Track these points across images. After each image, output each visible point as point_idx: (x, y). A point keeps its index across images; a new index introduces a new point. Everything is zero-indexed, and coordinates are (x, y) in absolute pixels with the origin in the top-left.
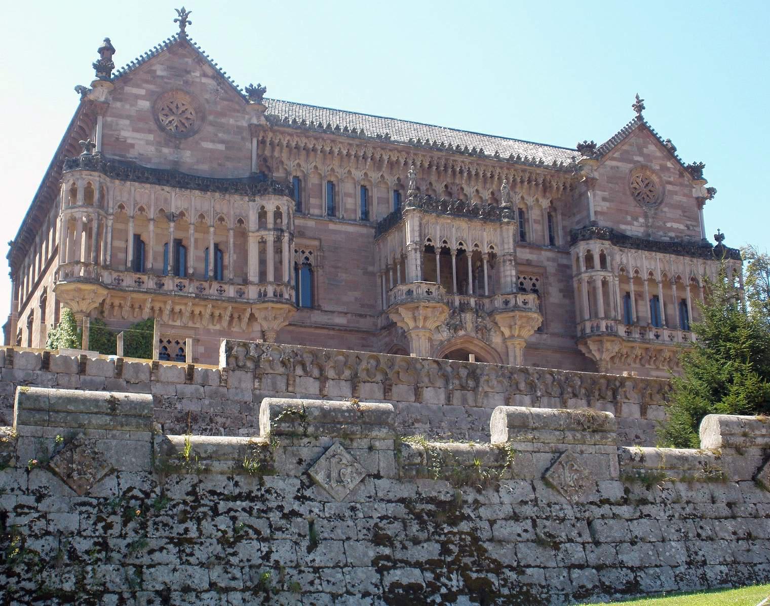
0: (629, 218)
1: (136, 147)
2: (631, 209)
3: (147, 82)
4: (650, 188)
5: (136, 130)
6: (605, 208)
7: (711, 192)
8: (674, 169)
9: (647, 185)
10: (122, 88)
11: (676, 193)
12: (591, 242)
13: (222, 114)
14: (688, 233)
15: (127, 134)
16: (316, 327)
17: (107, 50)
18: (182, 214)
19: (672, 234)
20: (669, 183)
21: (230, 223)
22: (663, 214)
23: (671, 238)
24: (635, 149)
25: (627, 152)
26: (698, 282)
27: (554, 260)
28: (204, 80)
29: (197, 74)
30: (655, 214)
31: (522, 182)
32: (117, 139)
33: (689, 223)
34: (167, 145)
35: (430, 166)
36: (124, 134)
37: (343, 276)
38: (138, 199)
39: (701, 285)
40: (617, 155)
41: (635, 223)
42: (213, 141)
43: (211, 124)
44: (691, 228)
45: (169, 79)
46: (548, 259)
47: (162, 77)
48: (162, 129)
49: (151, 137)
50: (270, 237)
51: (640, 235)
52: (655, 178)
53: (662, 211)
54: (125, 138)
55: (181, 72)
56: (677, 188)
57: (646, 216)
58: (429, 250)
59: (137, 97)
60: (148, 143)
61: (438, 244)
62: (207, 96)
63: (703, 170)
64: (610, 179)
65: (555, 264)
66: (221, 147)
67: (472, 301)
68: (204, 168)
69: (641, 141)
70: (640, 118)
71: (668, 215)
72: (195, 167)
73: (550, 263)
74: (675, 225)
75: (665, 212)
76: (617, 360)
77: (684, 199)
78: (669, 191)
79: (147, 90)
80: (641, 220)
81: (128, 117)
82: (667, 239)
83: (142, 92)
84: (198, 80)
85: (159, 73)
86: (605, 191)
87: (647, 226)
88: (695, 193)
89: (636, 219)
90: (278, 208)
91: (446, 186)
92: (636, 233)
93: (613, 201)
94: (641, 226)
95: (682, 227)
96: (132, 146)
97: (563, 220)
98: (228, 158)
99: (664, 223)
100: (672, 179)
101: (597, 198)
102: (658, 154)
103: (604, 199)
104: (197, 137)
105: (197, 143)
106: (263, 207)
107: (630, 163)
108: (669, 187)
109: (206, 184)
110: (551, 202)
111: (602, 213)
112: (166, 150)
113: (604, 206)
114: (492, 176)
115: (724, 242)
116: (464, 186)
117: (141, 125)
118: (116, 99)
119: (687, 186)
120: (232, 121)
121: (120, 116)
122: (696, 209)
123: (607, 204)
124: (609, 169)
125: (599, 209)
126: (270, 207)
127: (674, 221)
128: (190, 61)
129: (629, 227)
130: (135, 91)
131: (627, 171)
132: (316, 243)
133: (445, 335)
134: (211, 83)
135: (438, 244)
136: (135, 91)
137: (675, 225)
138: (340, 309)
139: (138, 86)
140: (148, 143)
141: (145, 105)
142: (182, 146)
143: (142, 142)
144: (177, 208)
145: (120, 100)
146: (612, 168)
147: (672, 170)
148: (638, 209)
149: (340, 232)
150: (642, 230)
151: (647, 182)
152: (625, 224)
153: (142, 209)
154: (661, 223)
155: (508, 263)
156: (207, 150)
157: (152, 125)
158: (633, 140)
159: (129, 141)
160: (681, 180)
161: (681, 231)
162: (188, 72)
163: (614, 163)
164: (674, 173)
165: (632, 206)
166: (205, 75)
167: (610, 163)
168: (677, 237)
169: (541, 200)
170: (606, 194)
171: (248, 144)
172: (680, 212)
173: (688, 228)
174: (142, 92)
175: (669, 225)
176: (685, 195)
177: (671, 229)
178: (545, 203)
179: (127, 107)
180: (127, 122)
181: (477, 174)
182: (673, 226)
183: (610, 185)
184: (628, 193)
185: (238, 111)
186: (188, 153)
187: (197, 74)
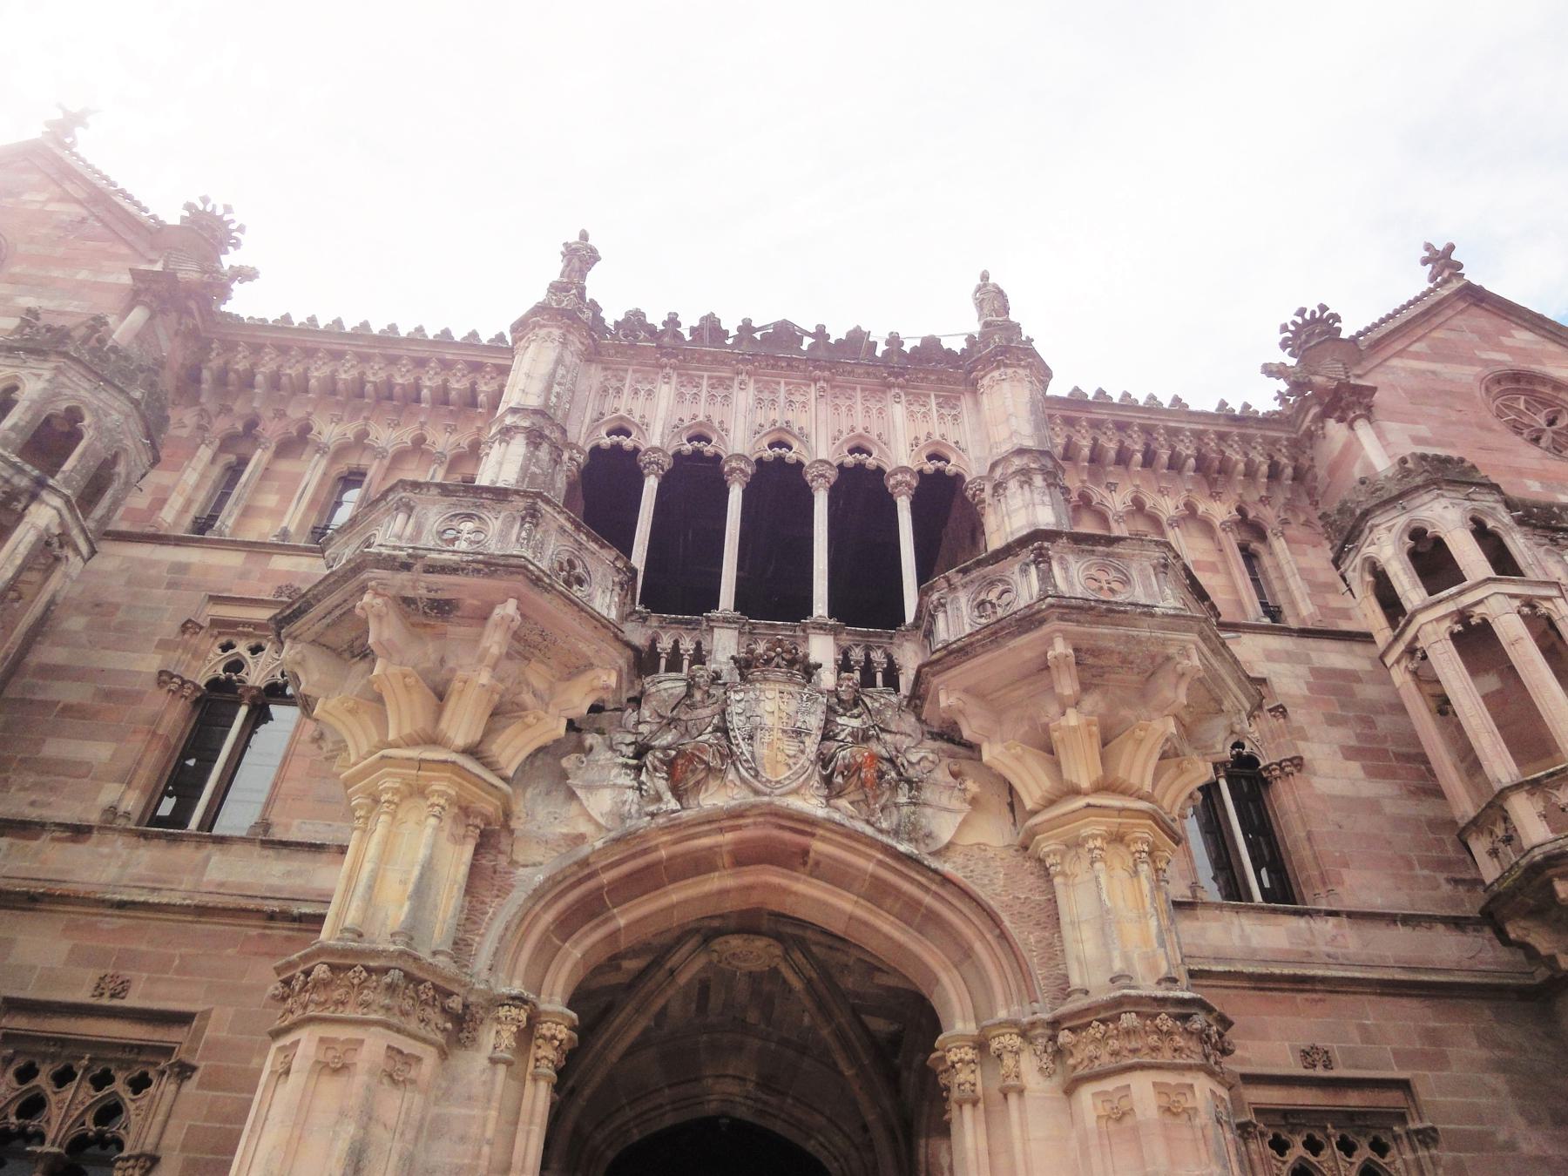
27: (1290, 657)
46: (1270, 656)
65: (1302, 670)
67: (821, 649)
73: (1277, 667)
133: (607, 800)
155: (1013, 485)
178: (1220, 511)
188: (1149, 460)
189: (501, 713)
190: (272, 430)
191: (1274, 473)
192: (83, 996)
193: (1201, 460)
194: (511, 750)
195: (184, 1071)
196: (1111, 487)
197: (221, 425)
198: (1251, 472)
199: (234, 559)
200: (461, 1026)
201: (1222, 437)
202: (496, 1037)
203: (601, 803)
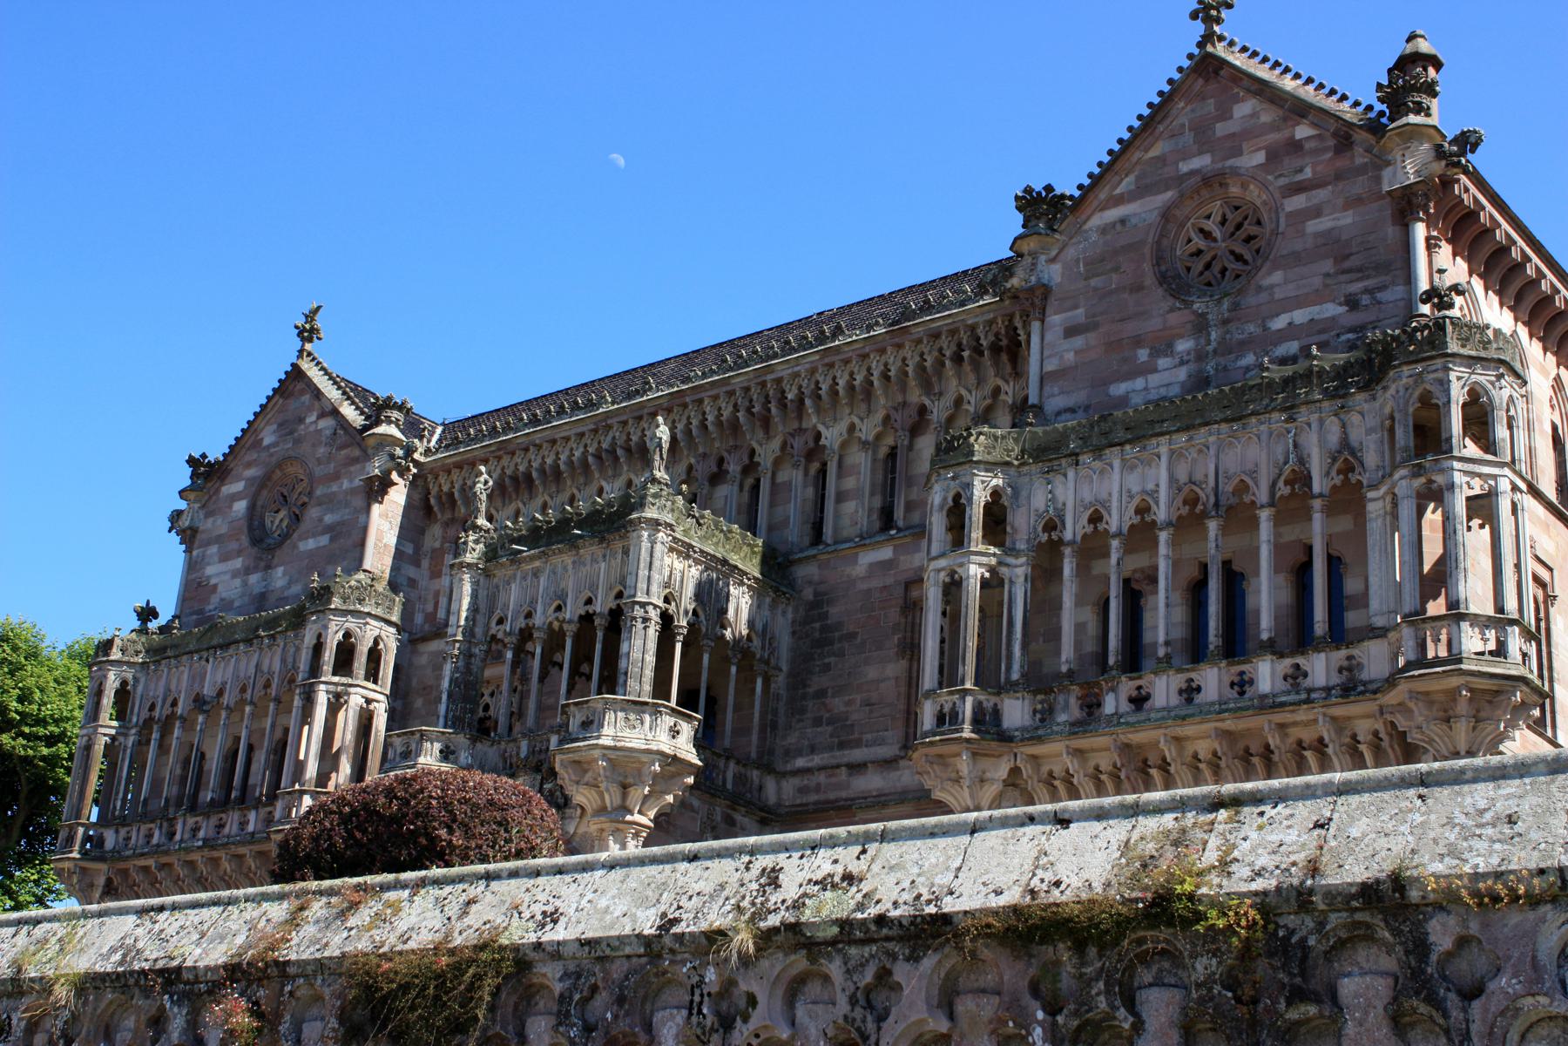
0: (1143, 354)
1: (220, 588)
2: (1155, 323)
3: (249, 465)
5: (224, 558)
6: (1070, 356)
11: (1317, 212)
13: (336, 477)
20: (1299, 188)
22: (1264, 297)
24: (1189, 137)
25: (1162, 160)
28: (322, 424)
30: (1235, 307)
32: (199, 584)
33: (1356, 287)
34: (256, 569)
40: (1127, 184)
41: (1163, 362)
49: (238, 563)
52: (1255, 194)
53: (1260, 289)
54: (209, 578)
56: (1322, 194)
57: (1200, 326)
59: (234, 498)
60: (235, 574)
64: (1095, 265)
66: (324, 540)
71: (1279, 294)
74: (1300, 316)
75: (1272, 287)
77: (1347, 219)
78: (1290, 215)
79: (248, 480)
92: (1153, 395)
94: (1182, 363)
95: (1332, 310)
100: (1308, 173)
101: (1048, 337)
103: (1071, 332)
105: (295, 547)
107: (1167, 189)
108: (1297, 202)
113: (1067, 352)
116: (821, 428)
117: (234, 546)
118: (208, 515)
119: (1362, 170)
120: (346, 484)
121: (208, 543)
122: (1392, 231)
123: (1078, 341)
124: (1094, 237)
125: (1050, 367)
129: (1139, 383)
131: (1153, 217)
141: (241, 506)
142: (276, 561)
146: (1104, 230)
147: (1307, 146)
148: (1174, 319)
150: (1182, 374)
154: (1251, 328)
157: (245, 540)
158: (1183, 113)
159: (213, 582)
160: (1341, 163)
162: (301, 420)
164: (1316, 152)
165: (1160, 312)
166: (322, 415)
167: (1097, 220)
170: (1079, 314)
172: (1328, 266)
173: (1352, 303)
175: (1279, 323)
176: (1354, 202)
177: (1291, 331)
181: (834, 392)
183: (1093, 282)
184: (1150, 280)
186: (280, 570)
193: (996, 349)
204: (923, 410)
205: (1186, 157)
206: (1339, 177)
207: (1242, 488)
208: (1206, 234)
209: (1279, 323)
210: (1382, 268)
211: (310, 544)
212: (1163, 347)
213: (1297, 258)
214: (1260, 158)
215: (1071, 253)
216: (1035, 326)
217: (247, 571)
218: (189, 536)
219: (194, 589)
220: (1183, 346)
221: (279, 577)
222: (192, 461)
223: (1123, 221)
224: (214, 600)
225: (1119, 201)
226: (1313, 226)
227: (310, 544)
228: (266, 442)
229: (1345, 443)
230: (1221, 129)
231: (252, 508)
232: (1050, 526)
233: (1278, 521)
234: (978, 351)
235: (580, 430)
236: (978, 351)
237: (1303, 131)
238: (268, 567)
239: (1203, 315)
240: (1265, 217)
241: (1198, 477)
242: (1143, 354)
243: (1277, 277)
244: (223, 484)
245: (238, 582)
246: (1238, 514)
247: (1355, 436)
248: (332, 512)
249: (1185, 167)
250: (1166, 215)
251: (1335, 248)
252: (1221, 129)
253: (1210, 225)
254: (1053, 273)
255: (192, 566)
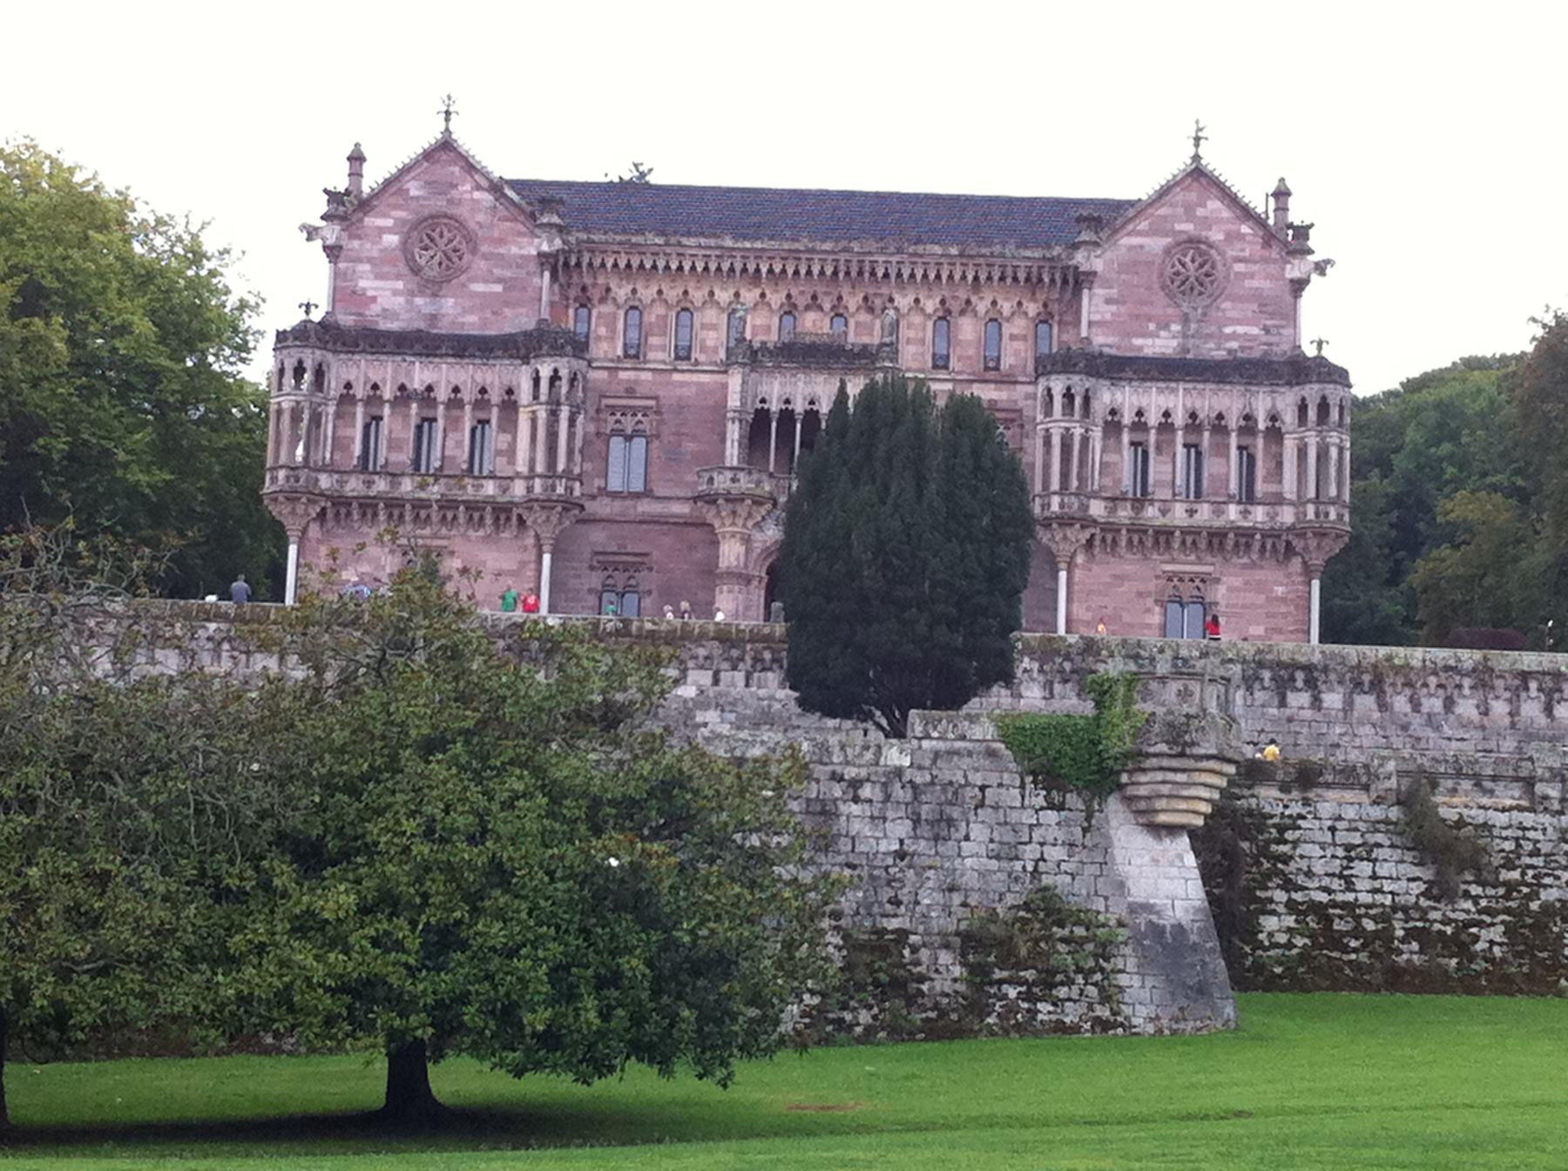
0: (1152, 326)
2: (1159, 311)
3: (396, 207)
4: (1207, 267)
5: (378, 277)
7: (1321, 268)
8: (1255, 235)
9: (1201, 266)
10: (361, 220)
11: (1252, 276)
12: (1053, 377)
13: (501, 241)
14: (1265, 339)
15: (366, 284)
16: (641, 522)
17: (357, 159)
18: (430, 388)
19: (1234, 345)
21: (495, 396)
23: (1230, 351)
24: (1180, 210)
25: (1165, 217)
26: (1256, 421)
28: (477, 195)
29: (468, 187)
30: (1205, 314)
31: (989, 278)
33: (1269, 323)
34: (422, 293)
35: (835, 273)
36: (362, 284)
37: (689, 446)
38: (370, 375)
39: (1261, 426)
40: (1143, 225)
41: (1163, 333)
42: (486, 281)
43: (485, 257)
44: (1273, 331)
45: (425, 199)
47: (417, 198)
48: (416, 270)
49: (400, 285)
50: (542, 415)
51: (1170, 351)
53: (1218, 308)
55: (441, 188)
56: (1255, 268)
57: (1185, 320)
58: (762, 416)
59: (382, 230)
60: (395, 293)
61: (775, 406)
62: (481, 217)
63: (1311, 232)
64: (1125, 267)
66: (498, 288)
68: (471, 323)
69: (1193, 196)
70: (1196, 158)
71: (1229, 314)
72: (461, 320)
74: (1240, 329)
76: (1097, 551)
77: (1267, 284)
80: (1175, 327)
81: (370, 260)
82: (1220, 354)
83: (389, 222)
84: (467, 196)
85: (413, 192)
86: (1111, 287)
87: (1185, 336)
88: (1294, 271)
89: (1166, 327)
90: (556, 371)
91: (866, 299)
92: (1157, 350)
93: (1124, 303)
95: (1255, 331)
96: (374, 299)
97: (1060, 331)
98: (507, 304)
99: (1220, 328)
100: (1247, 254)
102: (1226, 214)
103: (1108, 301)
104: (463, 278)
105: (464, 285)
106: (537, 372)
107: (1167, 235)
109: (465, 347)
110: (1045, 305)
111: (1100, 324)
112: (419, 301)
113: (1107, 312)
114: (938, 277)
115: (1325, 353)
117: (386, 269)
118: (351, 237)
119: (1275, 261)
120: (514, 250)
122: (1289, 298)
123: (1114, 308)
124: (1124, 250)
125: (1097, 317)
126: (545, 372)
127: (1239, 322)
128: (457, 169)
129: (1149, 341)
130: (381, 222)
132: (652, 403)
134: (486, 198)
135: (775, 406)
136: (381, 222)
137: (1240, 329)
138: (681, 495)
139: (385, 216)
140: (395, 293)
141: (392, 240)
143: (388, 293)
144: (422, 381)
145: (359, 237)
146: (1130, 248)
148: (1170, 311)
149: (687, 384)
150: (1174, 343)
151: (1199, 260)
152: (1144, 335)
153: (375, 387)
154: (1213, 328)
156: (477, 294)
157: (402, 268)
158: (1179, 196)
159: (370, 293)
160: (1266, 253)
161: (1254, 338)
163: (1135, 241)
166: (478, 188)
167: (1126, 241)
168: (1242, 348)
169: (1025, 304)
170: (1114, 292)
171: (536, 280)
172: (1255, 307)
173: (1267, 330)
174: (389, 222)
175: (1228, 330)
176: (1268, 277)
177: (1234, 337)
178: (1032, 308)
179: (368, 246)
180: (367, 267)
182: (1238, 332)
183: (1123, 276)
184: (1156, 286)
185: (524, 235)
186: (451, 301)
187: (468, 187)
188: (1002, 279)
189: (750, 515)
190: (595, 294)
191: (1065, 282)
192: (615, 549)
193: (1028, 280)
194: (750, 524)
195: (651, 569)
196: (982, 298)
197: (573, 293)
198: (1053, 281)
199: (604, 375)
200: (748, 580)
201: (1040, 268)
202: (755, 583)
203: (770, 533)
204: (968, 302)
205: (1180, 222)
206: (1265, 260)
207: (1220, 416)
208: (1183, 265)
209: (1228, 330)
210: (1284, 316)
211: (479, 287)
212: (1166, 327)
213: (1235, 299)
214: (1221, 237)
215: (1109, 255)
216: (1086, 291)
217: (411, 294)
218: (333, 252)
219: (342, 292)
220: (1175, 327)
221: (448, 305)
222: (326, 191)
223: (1141, 247)
224: (375, 309)
225: (1139, 234)
226: (1248, 283)
227: (479, 287)
228: (413, 192)
229: (1274, 406)
230: (1200, 212)
231: (404, 243)
232: (1113, 412)
233: (1239, 435)
234: (1015, 279)
235: (708, 252)
236: (1015, 279)
237: (1245, 229)
238: (435, 295)
239: (1186, 314)
240: (1219, 266)
241: (1198, 405)
242: (1152, 326)
243: (1227, 305)
244: (365, 214)
245: (401, 300)
246: (1219, 426)
247: (1280, 405)
248: (503, 267)
249: (1178, 227)
250: (1168, 251)
251: (1257, 296)
252: (1200, 212)
253: (1187, 260)
254: (1098, 265)
255: (337, 275)
